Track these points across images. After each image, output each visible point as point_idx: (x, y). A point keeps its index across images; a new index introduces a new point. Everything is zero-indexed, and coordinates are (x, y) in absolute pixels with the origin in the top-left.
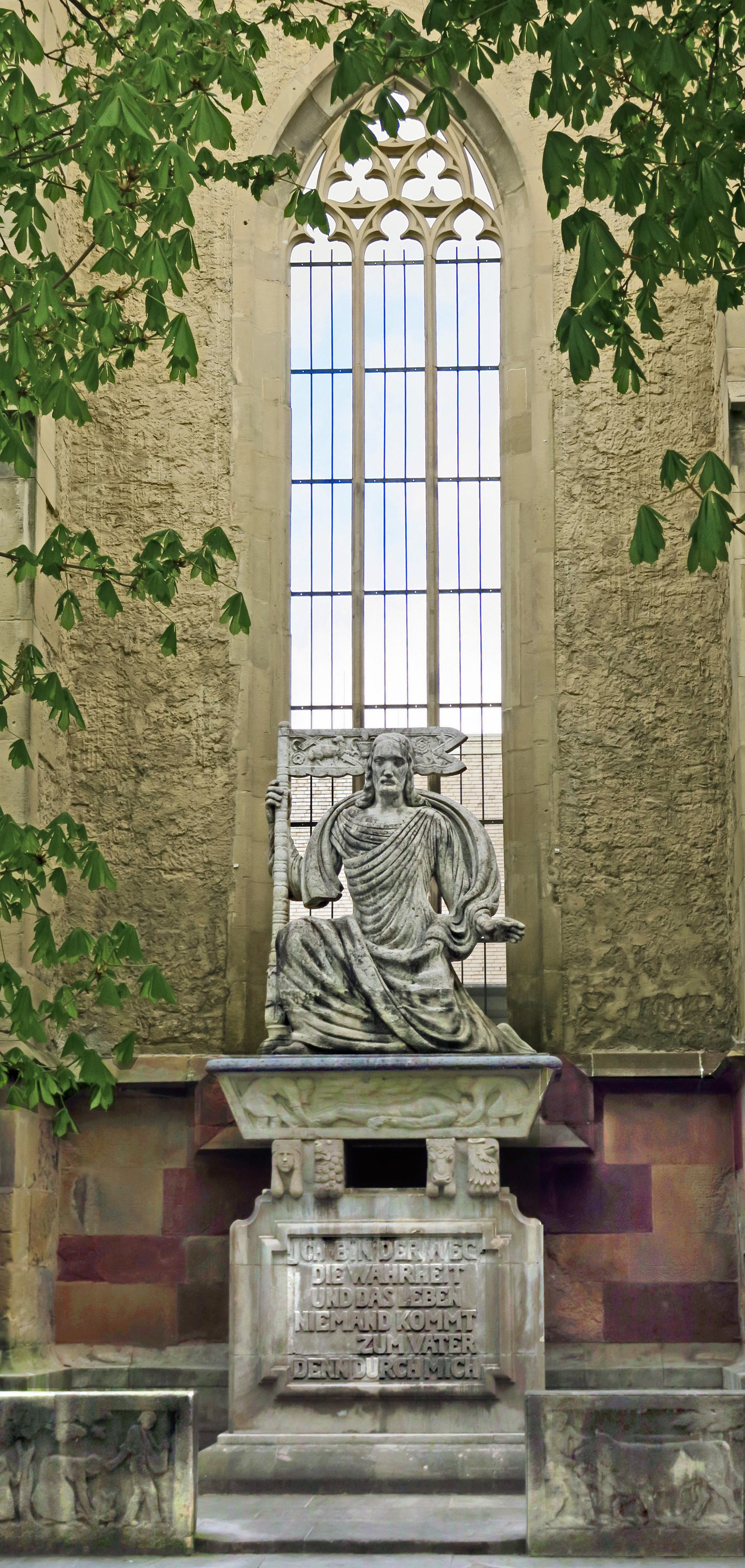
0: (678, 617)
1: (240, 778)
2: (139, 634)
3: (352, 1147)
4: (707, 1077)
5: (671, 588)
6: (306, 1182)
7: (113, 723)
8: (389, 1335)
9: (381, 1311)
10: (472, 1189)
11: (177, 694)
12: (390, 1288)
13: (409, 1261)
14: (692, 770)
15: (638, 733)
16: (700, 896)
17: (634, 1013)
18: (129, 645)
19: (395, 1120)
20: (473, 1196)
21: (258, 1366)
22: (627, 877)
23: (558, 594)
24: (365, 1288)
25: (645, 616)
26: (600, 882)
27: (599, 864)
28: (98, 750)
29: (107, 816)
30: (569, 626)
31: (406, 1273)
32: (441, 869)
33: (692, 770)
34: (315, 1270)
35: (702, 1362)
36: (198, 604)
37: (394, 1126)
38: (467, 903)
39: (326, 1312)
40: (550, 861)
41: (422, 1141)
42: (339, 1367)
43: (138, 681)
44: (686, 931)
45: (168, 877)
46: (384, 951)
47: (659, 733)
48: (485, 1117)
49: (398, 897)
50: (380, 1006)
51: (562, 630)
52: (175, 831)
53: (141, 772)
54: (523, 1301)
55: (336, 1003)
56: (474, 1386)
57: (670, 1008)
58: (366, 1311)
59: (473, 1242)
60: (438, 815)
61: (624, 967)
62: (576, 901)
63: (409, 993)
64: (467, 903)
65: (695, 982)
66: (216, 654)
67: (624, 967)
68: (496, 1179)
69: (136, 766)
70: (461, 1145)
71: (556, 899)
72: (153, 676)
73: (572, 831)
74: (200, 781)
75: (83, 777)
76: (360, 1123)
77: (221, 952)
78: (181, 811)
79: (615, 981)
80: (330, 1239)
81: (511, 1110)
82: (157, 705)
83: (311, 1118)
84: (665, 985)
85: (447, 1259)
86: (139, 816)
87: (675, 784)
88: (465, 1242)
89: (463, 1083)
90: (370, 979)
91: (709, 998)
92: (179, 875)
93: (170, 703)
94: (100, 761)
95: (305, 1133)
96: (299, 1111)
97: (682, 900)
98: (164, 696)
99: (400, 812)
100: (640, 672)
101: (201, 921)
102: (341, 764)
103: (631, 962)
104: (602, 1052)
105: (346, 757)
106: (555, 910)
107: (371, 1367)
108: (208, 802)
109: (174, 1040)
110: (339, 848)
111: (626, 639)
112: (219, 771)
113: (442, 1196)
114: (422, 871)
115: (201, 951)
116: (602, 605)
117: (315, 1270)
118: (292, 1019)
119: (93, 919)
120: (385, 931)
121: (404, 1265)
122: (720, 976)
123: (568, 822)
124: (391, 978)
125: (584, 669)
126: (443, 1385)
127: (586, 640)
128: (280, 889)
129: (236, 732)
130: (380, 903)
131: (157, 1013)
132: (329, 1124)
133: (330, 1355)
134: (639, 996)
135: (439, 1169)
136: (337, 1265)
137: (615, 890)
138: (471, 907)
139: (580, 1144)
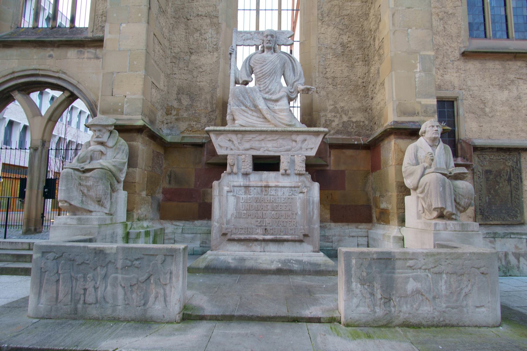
0: (355, 13)
1: (221, 56)
2: (192, 14)
3: (255, 158)
4: (364, 144)
5: (353, 5)
6: (238, 168)
7: (183, 39)
8: (267, 220)
9: (264, 212)
10: (296, 172)
11: (203, 31)
12: (268, 204)
13: (273, 195)
14: (359, 56)
15: (342, 45)
16: (361, 92)
17: (341, 126)
18: (189, 17)
19: (270, 149)
20: (296, 174)
21: (221, 228)
22: (339, 86)
23: (318, 6)
24: (258, 204)
25: (345, 12)
26: (331, 88)
27: (330, 82)
28: (179, 47)
29: (181, 66)
30: (322, 15)
31: (273, 200)
32: (286, 73)
33: (359, 56)
34: (241, 198)
35: (361, 229)
36: (210, 6)
37: (269, 151)
38: (295, 82)
39: (245, 212)
40: (315, 81)
41: (279, 156)
42: (249, 230)
43: (191, 27)
44: (357, 102)
45: (199, 84)
46: (267, 96)
47: (349, 45)
48: (301, 148)
49: (272, 79)
50: (264, 112)
51: (320, 15)
52: (201, 70)
53: (191, 53)
54: (313, 209)
55: (250, 112)
56: (297, 237)
57: (352, 125)
58: (259, 212)
59: (296, 189)
60: (284, 56)
61: (338, 112)
62: (323, 93)
63: (275, 110)
64: (295, 82)
65: (359, 117)
66: (215, 20)
67: (338, 112)
68: (305, 169)
69: (190, 52)
70: (292, 157)
71: (317, 92)
72: (196, 26)
73: (322, 73)
74: (209, 56)
75: (174, 54)
76: (258, 149)
77: (214, 106)
78: (204, 65)
79: (335, 116)
80: (247, 187)
81: (309, 146)
82: (197, 35)
83: (241, 148)
84: (350, 118)
85: (288, 194)
86: (190, 66)
87: (353, 60)
88: (293, 189)
89: (294, 137)
90: (262, 105)
91: (363, 122)
92: (202, 83)
93: (201, 34)
94: (179, 50)
95: (238, 152)
96: (237, 145)
97: (355, 93)
98: (199, 32)
99: (272, 54)
100: (343, 28)
101: (208, 97)
102: (253, 42)
103: (340, 111)
104: (331, 137)
105: (255, 39)
106: (317, 95)
107: (259, 231)
108: (212, 62)
109: (199, 131)
110: (252, 65)
111: (339, 19)
112: (215, 53)
113: (286, 174)
114: (279, 72)
115: (209, 105)
116: (332, 9)
117: (241, 198)
118: (236, 117)
119: (175, 95)
120: (267, 90)
121: (272, 197)
122: (367, 116)
123: (321, 70)
124: (269, 105)
125: (326, 26)
126: (285, 237)
127: (327, 19)
128: (232, 79)
129: (220, 43)
130: (266, 81)
131: (194, 123)
132: (247, 150)
133: (246, 226)
134: (342, 121)
135: (284, 165)
136: (249, 196)
137: (335, 90)
138: (295, 83)
139: (325, 163)
